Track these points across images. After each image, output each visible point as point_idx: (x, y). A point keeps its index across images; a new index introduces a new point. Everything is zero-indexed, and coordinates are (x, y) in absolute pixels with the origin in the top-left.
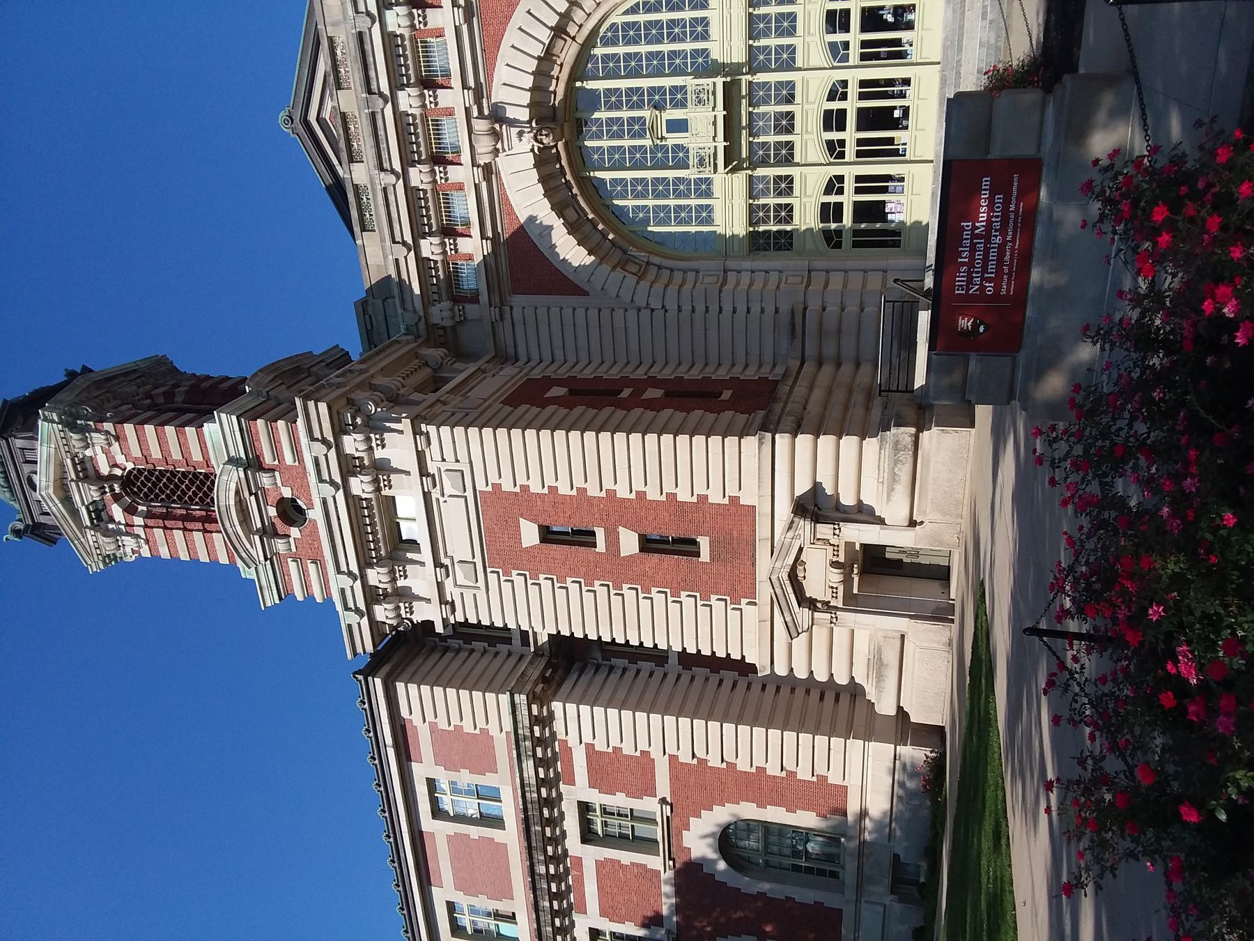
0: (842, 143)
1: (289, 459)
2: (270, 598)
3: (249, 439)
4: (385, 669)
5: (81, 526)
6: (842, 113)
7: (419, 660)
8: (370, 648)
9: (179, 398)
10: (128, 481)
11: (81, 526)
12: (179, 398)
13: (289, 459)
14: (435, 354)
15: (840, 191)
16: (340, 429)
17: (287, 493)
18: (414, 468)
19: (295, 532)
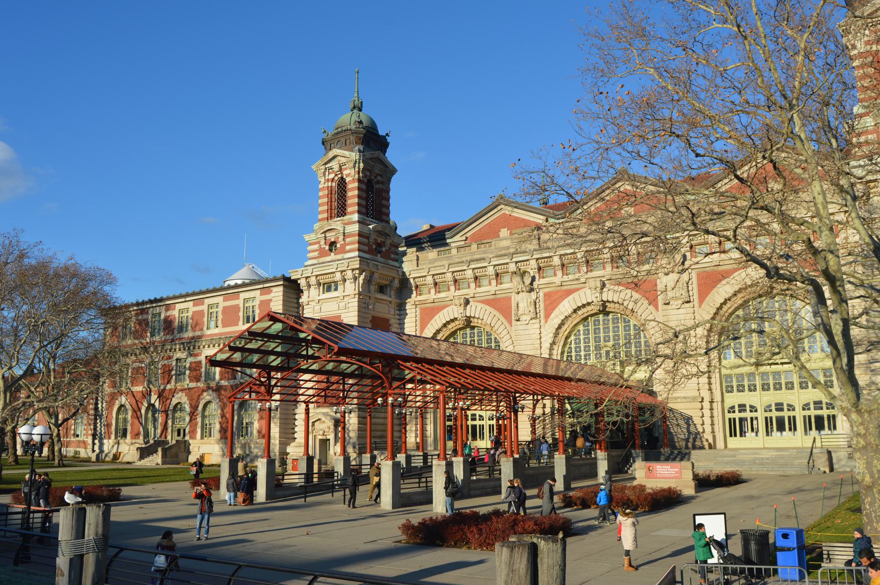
0: (734, 412)
1: (348, 248)
2: (307, 238)
3: (351, 235)
4: (286, 283)
5: (325, 164)
6: (782, 410)
7: (292, 291)
8: (293, 278)
9: (377, 186)
10: (342, 178)
11: (325, 164)
12: (377, 186)
13: (348, 248)
14: (396, 283)
15: (751, 411)
16: (353, 270)
17: (338, 245)
18: (345, 294)
19: (327, 248)
